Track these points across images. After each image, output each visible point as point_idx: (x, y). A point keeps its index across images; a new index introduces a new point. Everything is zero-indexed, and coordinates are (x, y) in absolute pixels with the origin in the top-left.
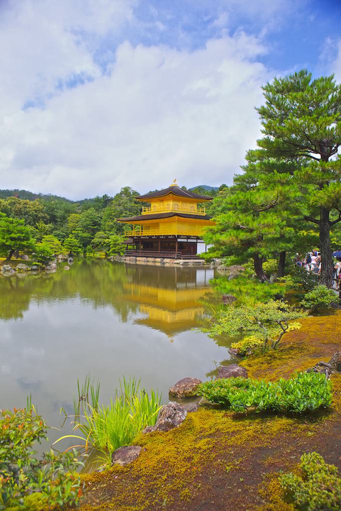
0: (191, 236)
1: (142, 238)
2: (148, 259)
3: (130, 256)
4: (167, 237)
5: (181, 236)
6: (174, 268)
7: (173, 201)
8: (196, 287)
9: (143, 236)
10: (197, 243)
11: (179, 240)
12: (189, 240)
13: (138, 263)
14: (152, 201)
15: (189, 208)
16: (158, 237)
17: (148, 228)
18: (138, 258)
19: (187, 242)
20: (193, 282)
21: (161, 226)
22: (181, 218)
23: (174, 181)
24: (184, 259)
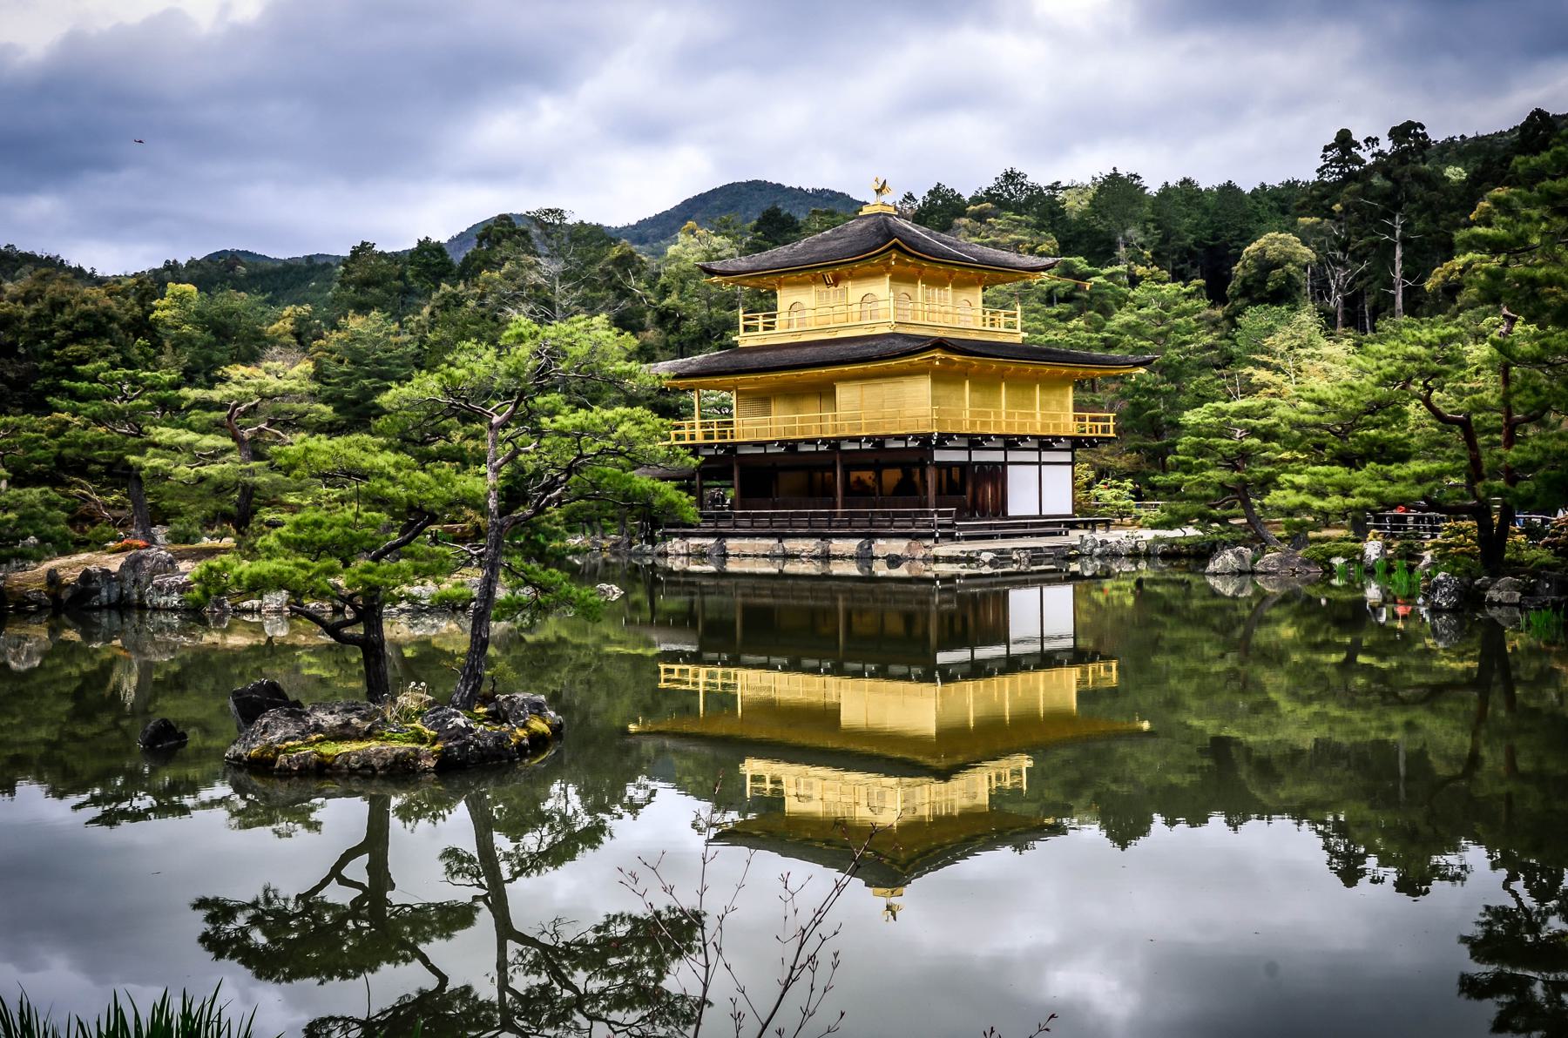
0: (987, 437)
1: (742, 451)
2: (791, 545)
3: (685, 536)
4: (879, 442)
5: (950, 436)
6: (931, 581)
8: (1013, 665)
10: (1005, 464)
11: (939, 456)
12: (978, 456)
13: (732, 566)
14: (780, 284)
15: (959, 312)
16: (834, 444)
17: (761, 399)
18: (732, 544)
20: (998, 644)
22: (956, 358)
23: (878, 191)
24: (968, 538)
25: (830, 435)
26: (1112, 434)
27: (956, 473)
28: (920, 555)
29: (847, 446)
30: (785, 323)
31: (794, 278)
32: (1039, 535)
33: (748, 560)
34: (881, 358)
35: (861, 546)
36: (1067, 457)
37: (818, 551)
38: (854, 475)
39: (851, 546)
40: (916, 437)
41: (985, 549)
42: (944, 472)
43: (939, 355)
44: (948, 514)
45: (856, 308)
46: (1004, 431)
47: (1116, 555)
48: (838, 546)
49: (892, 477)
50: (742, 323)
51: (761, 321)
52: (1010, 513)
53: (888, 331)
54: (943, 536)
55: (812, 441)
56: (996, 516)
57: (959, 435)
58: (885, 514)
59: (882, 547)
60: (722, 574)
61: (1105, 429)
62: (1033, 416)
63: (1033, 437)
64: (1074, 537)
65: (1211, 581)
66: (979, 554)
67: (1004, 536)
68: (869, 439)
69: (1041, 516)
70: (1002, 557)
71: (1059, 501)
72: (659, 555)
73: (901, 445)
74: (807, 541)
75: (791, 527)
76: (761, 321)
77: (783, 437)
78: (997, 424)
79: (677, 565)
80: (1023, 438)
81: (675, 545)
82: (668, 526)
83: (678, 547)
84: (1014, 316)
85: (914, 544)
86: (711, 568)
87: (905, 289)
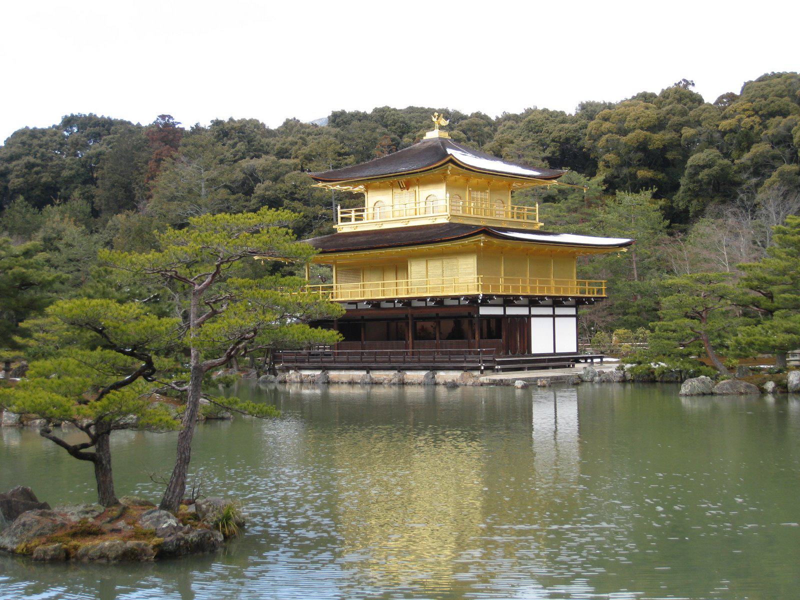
0: (517, 297)
2: (377, 375)
4: (439, 301)
5: (490, 297)
7: (447, 186)
9: (351, 303)
10: (529, 317)
11: (484, 311)
12: (511, 311)
13: (333, 391)
14: (367, 188)
16: (407, 302)
17: (355, 271)
18: (333, 374)
19: (505, 317)
21: (416, 269)
22: (495, 241)
24: (504, 370)
25: (404, 295)
26: (604, 295)
27: (493, 324)
28: (470, 382)
29: (415, 304)
30: (370, 217)
31: (377, 183)
32: (554, 367)
33: (345, 386)
35: (426, 376)
36: (572, 311)
37: (396, 380)
38: (419, 325)
39: (420, 375)
40: (467, 297)
41: (518, 377)
42: (485, 323)
43: (482, 238)
44: (490, 352)
45: (422, 205)
46: (529, 293)
47: (609, 381)
48: (411, 375)
49: (448, 326)
50: (339, 216)
52: (535, 350)
54: (486, 368)
55: (391, 301)
56: (523, 354)
57: (498, 296)
58: (443, 353)
59: (443, 376)
60: (325, 397)
61: (599, 291)
62: (547, 282)
63: (549, 297)
64: (580, 368)
65: (683, 400)
66: (514, 380)
67: (530, 369)
68: (433, 299)
69: (555, 354)
70: (529, 385)
71: (567, 343)
72: (280, 382)
73: (456, 302)
74: (387, 373)
75: (376, 362)
76: (353, 214)
77: (370, 298)
78: (524, 288)
79: (292, 389)
80: (542, 298)
81: (292, 375)
82: (285, 362)
83: (293, 376)
84: (535, 211)
85: (467, 374)
86: (318, 392)
87: (455, 191)
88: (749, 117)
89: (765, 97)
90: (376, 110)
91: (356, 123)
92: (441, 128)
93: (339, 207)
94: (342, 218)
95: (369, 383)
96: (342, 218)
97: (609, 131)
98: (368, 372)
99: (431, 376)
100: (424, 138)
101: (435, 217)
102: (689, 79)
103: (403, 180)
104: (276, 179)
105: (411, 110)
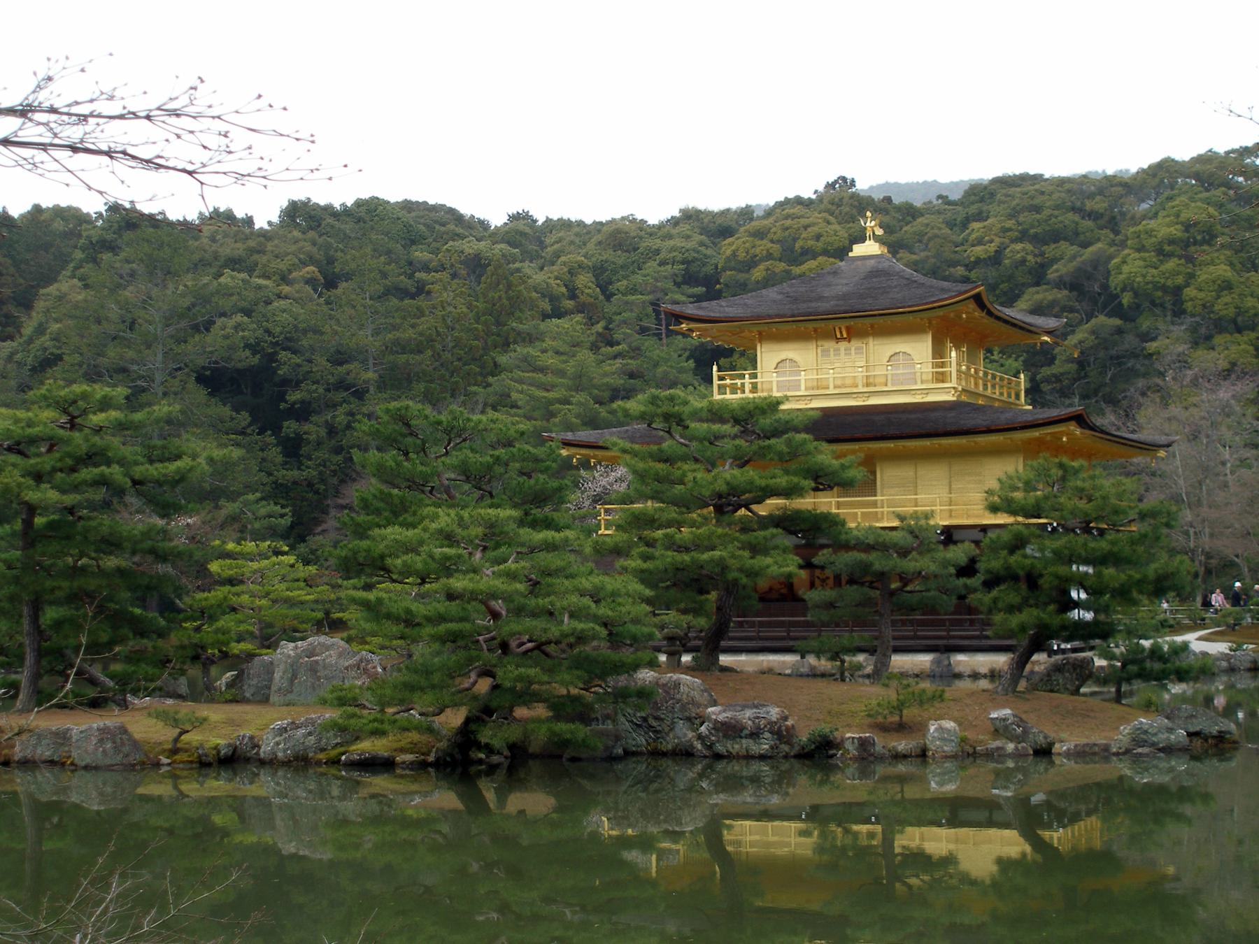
34: (989, 431)
51: (747, 380)
53: (949, 397)
88: (1013, 241)
89: (1037, 209)
90: (359, 203)
91: (330, 220)
92: (877, 239)
93: (715, 368)
94: (719, 386)
95: (808, 676)
96: (719, 386)
97: (769, 256)
98: (803, 657)
99: (946, 663)
100: (850, 254)
101: (928, 391)
102: (849, 177)
103: (843, 325)
104: (248, 313)
105: (408, 205)
